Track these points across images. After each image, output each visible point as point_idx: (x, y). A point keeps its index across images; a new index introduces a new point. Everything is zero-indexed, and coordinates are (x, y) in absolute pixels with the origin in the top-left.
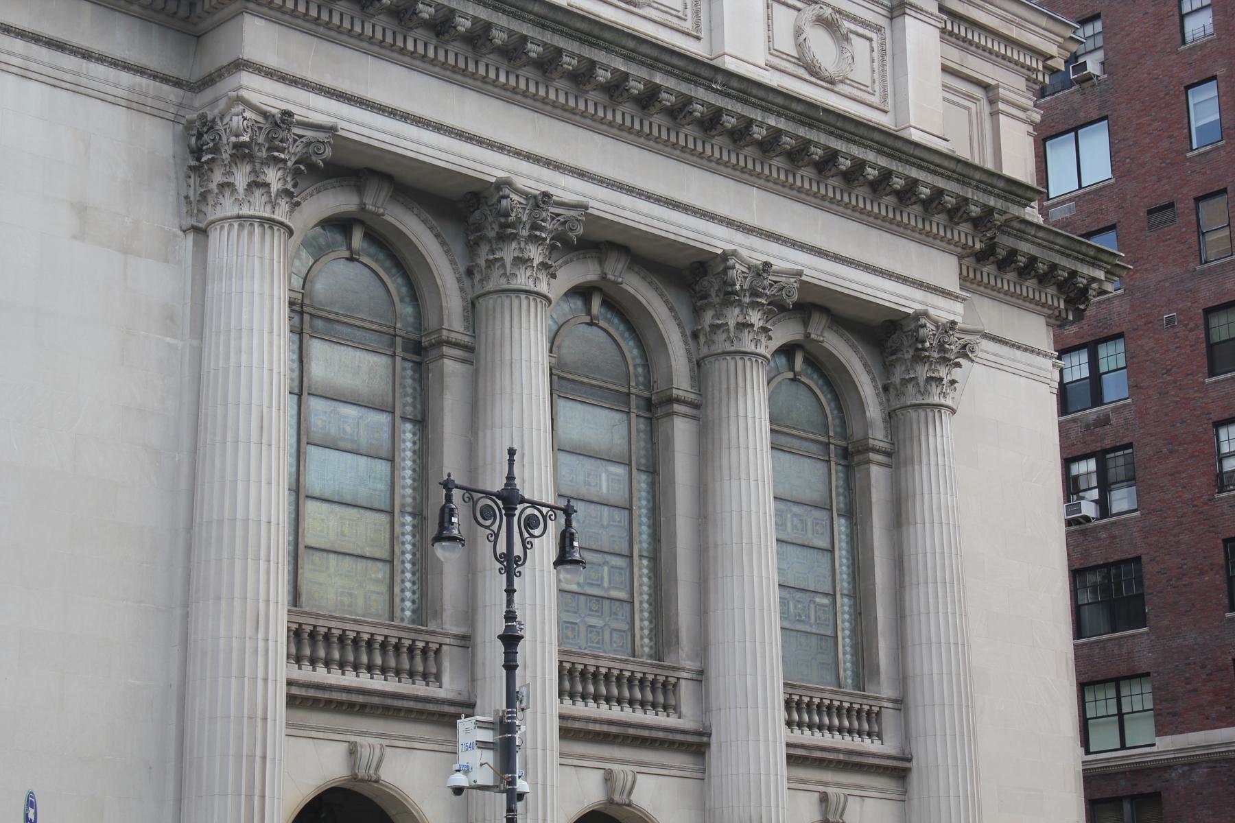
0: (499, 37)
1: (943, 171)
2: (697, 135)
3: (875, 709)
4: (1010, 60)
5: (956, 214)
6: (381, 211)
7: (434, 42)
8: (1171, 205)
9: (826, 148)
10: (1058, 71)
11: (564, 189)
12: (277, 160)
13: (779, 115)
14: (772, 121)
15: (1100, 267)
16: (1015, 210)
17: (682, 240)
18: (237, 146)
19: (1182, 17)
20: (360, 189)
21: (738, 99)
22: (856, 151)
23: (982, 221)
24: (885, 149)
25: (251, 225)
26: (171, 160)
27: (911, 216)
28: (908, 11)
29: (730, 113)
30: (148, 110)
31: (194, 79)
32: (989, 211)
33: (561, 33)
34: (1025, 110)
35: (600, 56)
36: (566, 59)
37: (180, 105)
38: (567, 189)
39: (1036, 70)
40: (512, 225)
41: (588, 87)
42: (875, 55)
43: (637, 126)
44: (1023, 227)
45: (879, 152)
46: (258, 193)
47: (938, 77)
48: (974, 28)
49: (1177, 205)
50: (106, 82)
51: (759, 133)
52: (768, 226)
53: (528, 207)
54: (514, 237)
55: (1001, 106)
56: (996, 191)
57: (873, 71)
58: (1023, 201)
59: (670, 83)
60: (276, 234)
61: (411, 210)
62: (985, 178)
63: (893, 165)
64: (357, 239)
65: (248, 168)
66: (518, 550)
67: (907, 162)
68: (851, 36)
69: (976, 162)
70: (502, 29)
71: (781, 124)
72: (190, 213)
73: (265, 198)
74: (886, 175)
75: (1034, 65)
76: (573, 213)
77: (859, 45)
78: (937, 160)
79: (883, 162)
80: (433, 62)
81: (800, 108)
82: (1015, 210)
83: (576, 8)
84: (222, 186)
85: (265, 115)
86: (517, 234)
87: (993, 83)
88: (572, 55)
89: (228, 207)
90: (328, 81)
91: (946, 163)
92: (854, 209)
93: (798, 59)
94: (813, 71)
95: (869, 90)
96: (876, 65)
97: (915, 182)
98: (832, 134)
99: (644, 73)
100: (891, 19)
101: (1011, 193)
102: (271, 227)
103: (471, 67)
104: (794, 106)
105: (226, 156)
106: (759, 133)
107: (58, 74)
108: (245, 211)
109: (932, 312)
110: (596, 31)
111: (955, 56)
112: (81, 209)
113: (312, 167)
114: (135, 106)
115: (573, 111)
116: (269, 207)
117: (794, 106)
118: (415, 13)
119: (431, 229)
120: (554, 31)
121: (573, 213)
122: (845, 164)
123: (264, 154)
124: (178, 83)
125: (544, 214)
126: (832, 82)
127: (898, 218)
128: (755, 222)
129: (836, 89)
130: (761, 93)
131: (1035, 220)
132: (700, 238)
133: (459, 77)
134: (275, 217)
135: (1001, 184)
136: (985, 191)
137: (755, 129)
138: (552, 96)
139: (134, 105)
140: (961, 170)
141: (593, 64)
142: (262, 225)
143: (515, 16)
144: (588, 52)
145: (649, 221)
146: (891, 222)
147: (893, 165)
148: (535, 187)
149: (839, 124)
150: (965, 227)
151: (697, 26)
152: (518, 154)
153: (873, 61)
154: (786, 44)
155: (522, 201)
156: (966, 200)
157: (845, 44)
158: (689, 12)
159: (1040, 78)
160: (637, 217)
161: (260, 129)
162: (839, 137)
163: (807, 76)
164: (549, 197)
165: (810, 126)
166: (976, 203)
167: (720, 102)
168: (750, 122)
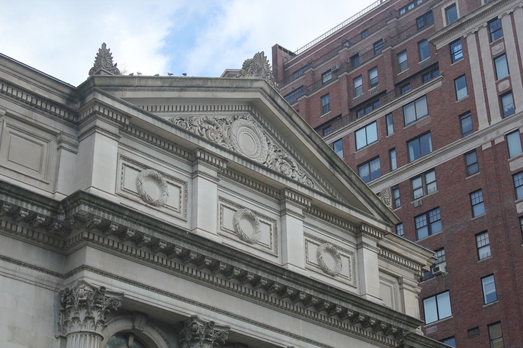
0: (193, 256)
1: (380, 313)
2: (276, 297)
5: (386, 331)
6: (142, 329)
7: (166, 258)
8: (477, 328)
9: (331, 303)
10: (427, 271)
11: (220, 320)
12: (98, 308)
13: (311, 289)
14: (308, 292)
16: (412, 330)
17: (270, 342)
18: (81, 301)
19: (478, 249)
20: (133, 320)
21: (294, 282)
22: (344, 304)
23: (398, 335)
24: (356, 304)
25: (86, 335)
26: (53, 307)
27: (367, 332)
28: (364, 246)
29: (290, 288)
30: (44, 286)
31: (64, 273)
32: (400, 330)
33: (219, 254)
34: (414, 287)
35: (235, 264)
36: (221, 265)
37: (58, 284)
38: (221, 320)
39: (418, 271)
40: (198, 336)
41: (230, 277)
42: (351, 264)
43: (251, 294)
44: (415, 337)
45: (353, 305)
46: (89, 321)
47: (377, 273)
48: (392, 253)
49: (480, 328)
50: (27, 275)
51: (302, 296)
52: (307, 336)
53: (204, 328)
54: (198, 341)
55: (404, 286)
56: (403, 322)
57: (350, 271)
58: (415, 326)
59: (265, 275)
60: (96, 339)
61: (154, 329)
62: (398, 316)
63: (360, 311)
64: (131, 342)
65: (85, 311)
67: (365, 309)
68: (341, 256)
69: (394, 309)
70: (195, 253)
71: (312, 293)
72: (60, 330)
73: (92, 324)
74: (357, 314)
75: (417, 269)
76: (223, 330)
77: (344, 260)
78: (378, 308)
79: (355, 309)
80: (165, 266)
81: (319, 286)
82: (412, 330)
83: (226, 244)
84: (74, 319)
85: (93, 288)
86: (199, 339)
87: (400, 276)
88: (224, 264)
89: (76, 327)
90: (121, 274)
91: (382, 310)
92: (343, 329)
93: (319, 266)
94: (325, 271)
95: (349, 278)
96: (351, 268)
97: (369, 318)
98: (333, 297)
99: (254, 271)
100: (357, 249)
101: (409, 322)
102: (94, 336)
103: (181, 269)
104: (317, 285)
105: (76, 306)
106: (302, 296)
107: (7, 271)
108: (83, 329)
110: (234, 254)
111: (384, 265)
112: (13, 329)
113: (112, 310)
114: (38, 284)
115: (224, 287)
116: (93, 328)
117: (317, 285)
118: (158, 246)
119: (163, 337)
120: (216, 254)
121: (223, 330)
122: (339, 310)
123: (92, 305)
124: (57, 275)
125: (211, 331)
126: (333, 275)
127: (362, 333)
128: (301, 334)
129: (335, 278)
130: (303, 280)
131: (420, 334)
132: (278, 341)
133: (176, 273)
134: (96, 332)
135: (405, 319)
136: (398, 322)
137: (301, 295)
138: (215, 281)
139: (38, 284)
140: (388, 313)
141: (232, 267)
142: (90, 335)
143: (200, 247)
144: (230, 263)
145: (256, 334)
146: (359, 334)
147: (360, 311)
148: (207, 319)
149: (336, 293)
150: (390, 337)
151: (276, 251)
152: (200, 305)
153: (350, 266)
154: (313, 259)
155: (202, 325)
156: (391, 325)
157: (338, 260)
158: (273, 246)
159: (420, 274)
160: (251, 332)
161: (91, 294)
162: (336, 298)
163: (322, 273)
164: (213, 324)
165: (324, 294)
166: (395, 327)
167: (286, 283)
168: (299, 292)
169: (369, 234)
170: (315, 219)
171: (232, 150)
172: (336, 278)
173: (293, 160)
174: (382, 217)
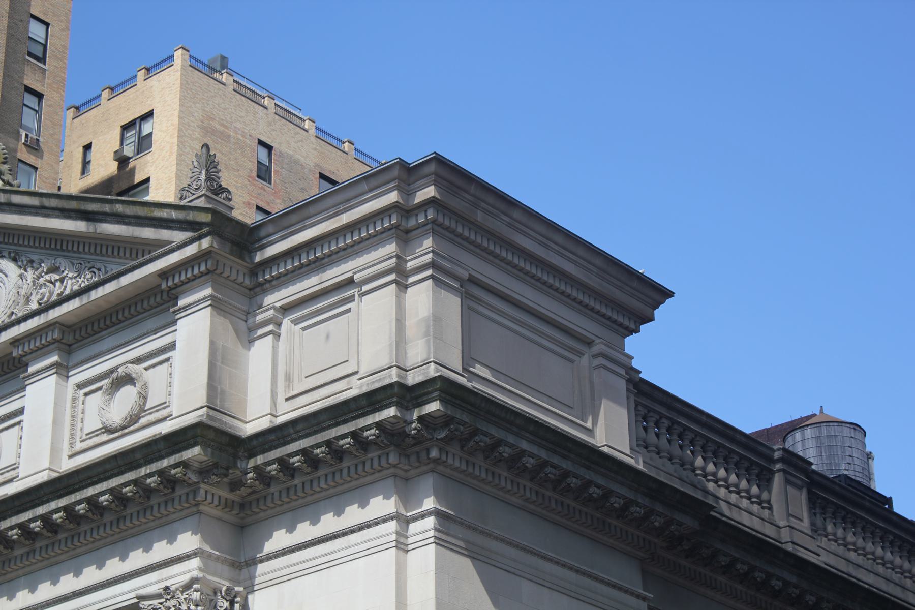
4: (362, 240)
15: (388, 406)
87: (349, 275)
109: (143, 592)
169: (183, 283)
170: (102, 339)
172: (143, 421)
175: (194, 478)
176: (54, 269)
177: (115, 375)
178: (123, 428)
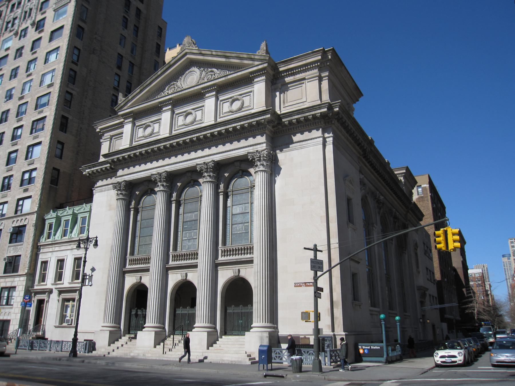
3: (251, 247)
66: (88, 247)
87: (304, 77)
171: (182, 89)
173: (213, 69)
174: (261, 61)
175: (266, 123)
176: (212, 71)
177: (146, 125)
178: (236, 111)
